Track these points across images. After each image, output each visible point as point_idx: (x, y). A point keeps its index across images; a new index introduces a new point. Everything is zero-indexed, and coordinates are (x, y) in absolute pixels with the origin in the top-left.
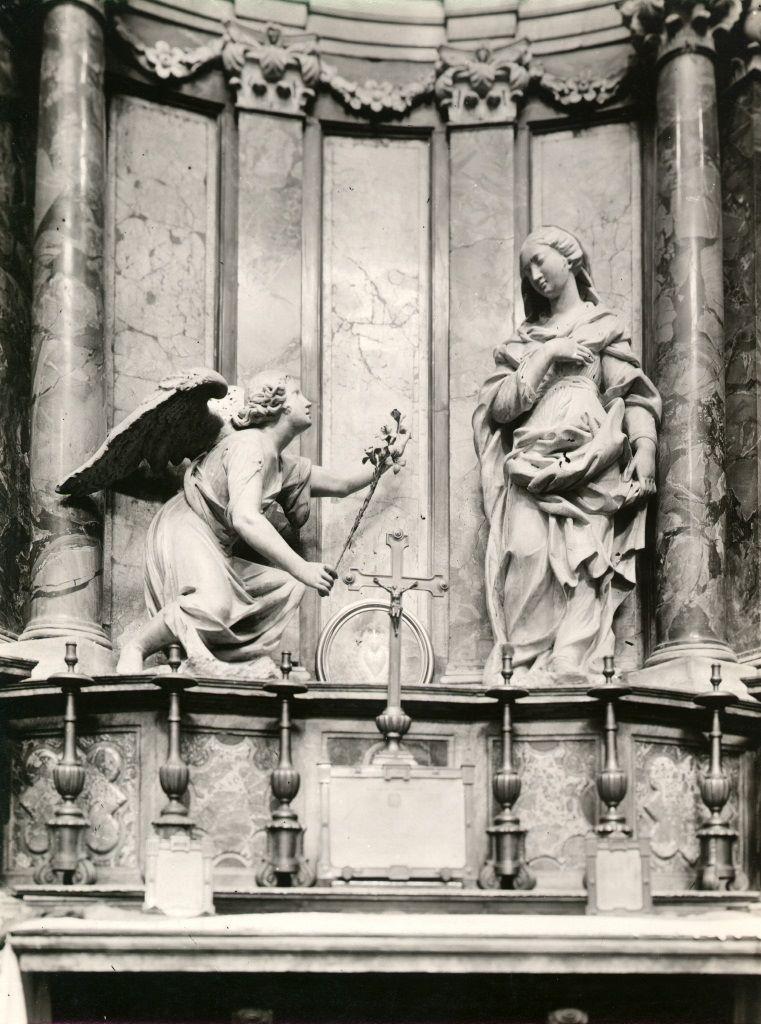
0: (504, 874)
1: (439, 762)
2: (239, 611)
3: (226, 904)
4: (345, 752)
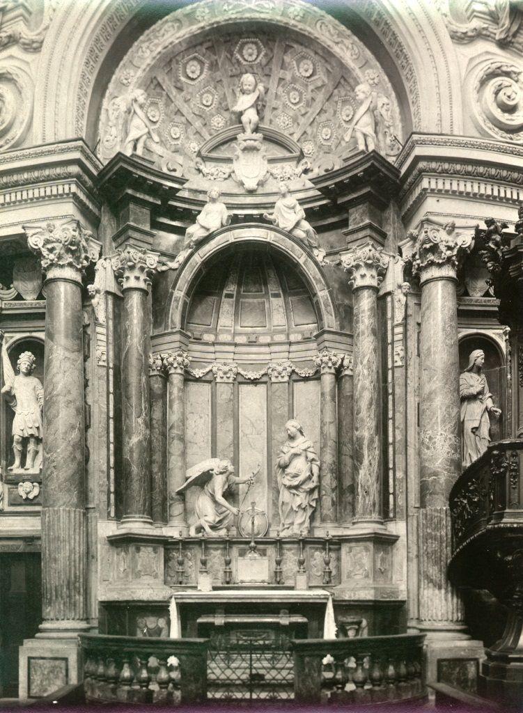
0: (278, 581)
1: (265, 555)
2: (218, 519)
3: (215, 589)
4: (242, 554)
